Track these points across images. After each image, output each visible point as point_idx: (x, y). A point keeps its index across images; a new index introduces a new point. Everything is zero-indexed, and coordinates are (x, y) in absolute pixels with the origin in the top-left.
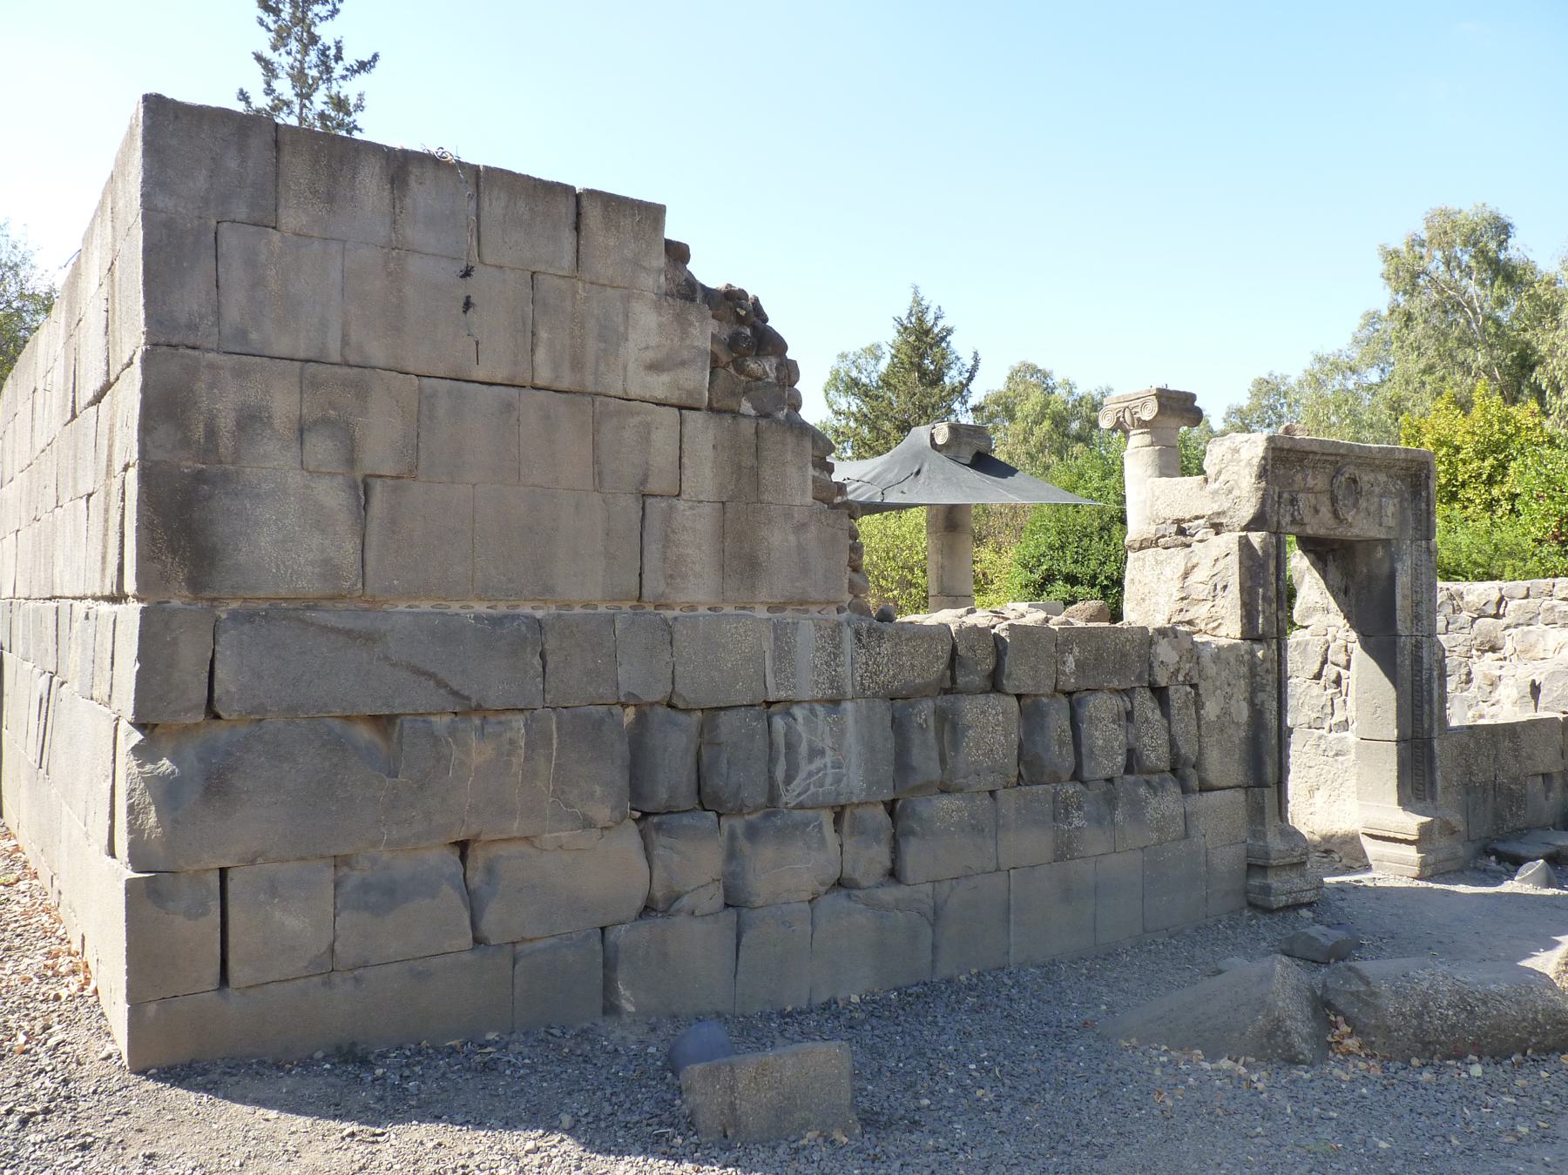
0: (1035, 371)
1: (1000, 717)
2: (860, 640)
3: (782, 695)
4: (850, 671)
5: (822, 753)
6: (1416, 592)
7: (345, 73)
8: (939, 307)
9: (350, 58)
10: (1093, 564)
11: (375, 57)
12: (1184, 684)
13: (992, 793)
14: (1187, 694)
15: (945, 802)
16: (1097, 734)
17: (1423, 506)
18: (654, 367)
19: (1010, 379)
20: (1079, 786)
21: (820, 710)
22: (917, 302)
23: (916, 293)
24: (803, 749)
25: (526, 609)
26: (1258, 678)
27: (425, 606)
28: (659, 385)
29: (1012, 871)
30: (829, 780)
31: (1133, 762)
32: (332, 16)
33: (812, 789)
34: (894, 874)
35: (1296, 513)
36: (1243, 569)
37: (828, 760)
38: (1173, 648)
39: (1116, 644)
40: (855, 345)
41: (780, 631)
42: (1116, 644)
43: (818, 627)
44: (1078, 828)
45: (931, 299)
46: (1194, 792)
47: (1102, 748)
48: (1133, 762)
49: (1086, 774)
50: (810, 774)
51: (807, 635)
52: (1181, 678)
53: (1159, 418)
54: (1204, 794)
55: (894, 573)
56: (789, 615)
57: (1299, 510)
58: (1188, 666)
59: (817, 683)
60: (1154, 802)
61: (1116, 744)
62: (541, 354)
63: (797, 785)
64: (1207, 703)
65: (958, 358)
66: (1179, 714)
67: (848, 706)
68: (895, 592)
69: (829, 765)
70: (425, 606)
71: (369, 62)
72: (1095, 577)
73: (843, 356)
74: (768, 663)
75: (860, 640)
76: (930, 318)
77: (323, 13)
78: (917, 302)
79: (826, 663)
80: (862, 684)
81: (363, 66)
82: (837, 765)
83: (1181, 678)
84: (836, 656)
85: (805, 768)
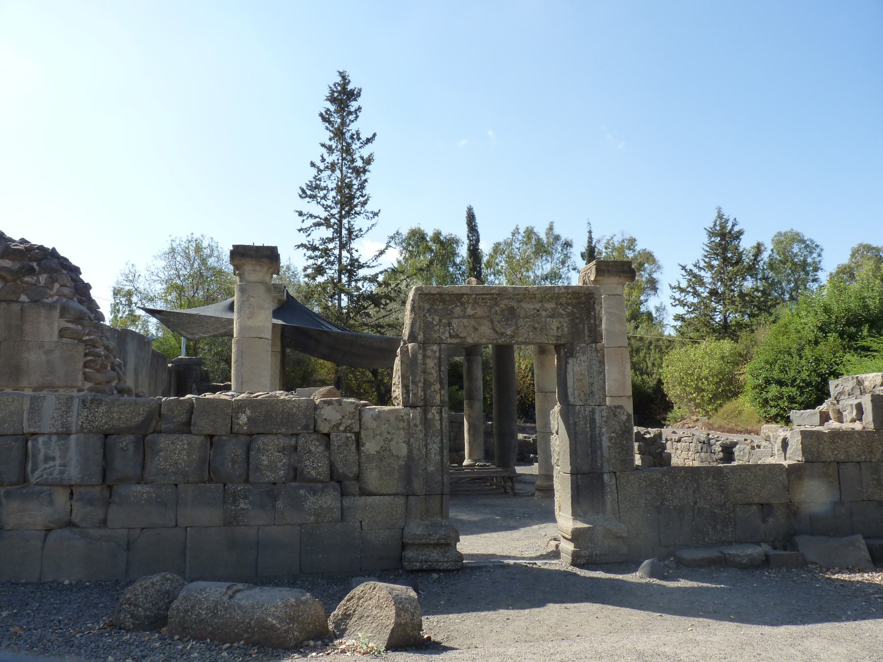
0: (868, 248)
1: (186, 446)
2: (85, 405)
3: (32, 430)
4: (76, 418)
5: (54, 459)
6: (591, 376)
7: (361, 145)
8: (735, 219)
9: (363, 137)
11: (374, 135)
12: (345, 431)
13: (176, 485)
14: (347, 438)
15: (139, 488)
16: (264, 458)
17: (592, 321)
19: (853, 255)
20: (247, 486)
21: (54, 438)
22: (720, 217)
23: (719, 212)
24: (41, 457)
26: (411, 429)
29: (188, 529)
30: (56, 472)
31: (296, 474)
32: (356, 119)
33: (45, 476)
34: (104, 523)
35: (451, 331)
36: (404, 366)
37: (58, 462)
38: (337, 411)
39: (283, 409)
41: (33, 400)
42: (283, 409)
43: (58, 398)
44: (243, 509)
45: (728, 213)
46: (355, 495)
47: (267, 466)
48: (296, 474)
49: (251, 479)
50: (45, 469)
51: (50, 403)
52: (342, 428)
53: (600, 278)
54: (363, 498)
55: (692, 383)
56: (44, 392)
57: (453, 329)
58: (349, 422)
59: (53, 425)
60: (313, 499)
61: (280, 465)
63: (37, 473)
64: (367, 444)
65: (817, 246)
66: (338, 449)
67: (73, 437)
69: (57, 465)
71: (371, 138)
72: (795, 380)
74: (25, 415)
75: (85, 405)
76: (730, 225)
78: (720, 217)
79: (61, 416)
80: (82, 426)
81: (368, 141)
82: (64, 465)
83: (342, 428)
84: (67, 412)
85: (42, 466)
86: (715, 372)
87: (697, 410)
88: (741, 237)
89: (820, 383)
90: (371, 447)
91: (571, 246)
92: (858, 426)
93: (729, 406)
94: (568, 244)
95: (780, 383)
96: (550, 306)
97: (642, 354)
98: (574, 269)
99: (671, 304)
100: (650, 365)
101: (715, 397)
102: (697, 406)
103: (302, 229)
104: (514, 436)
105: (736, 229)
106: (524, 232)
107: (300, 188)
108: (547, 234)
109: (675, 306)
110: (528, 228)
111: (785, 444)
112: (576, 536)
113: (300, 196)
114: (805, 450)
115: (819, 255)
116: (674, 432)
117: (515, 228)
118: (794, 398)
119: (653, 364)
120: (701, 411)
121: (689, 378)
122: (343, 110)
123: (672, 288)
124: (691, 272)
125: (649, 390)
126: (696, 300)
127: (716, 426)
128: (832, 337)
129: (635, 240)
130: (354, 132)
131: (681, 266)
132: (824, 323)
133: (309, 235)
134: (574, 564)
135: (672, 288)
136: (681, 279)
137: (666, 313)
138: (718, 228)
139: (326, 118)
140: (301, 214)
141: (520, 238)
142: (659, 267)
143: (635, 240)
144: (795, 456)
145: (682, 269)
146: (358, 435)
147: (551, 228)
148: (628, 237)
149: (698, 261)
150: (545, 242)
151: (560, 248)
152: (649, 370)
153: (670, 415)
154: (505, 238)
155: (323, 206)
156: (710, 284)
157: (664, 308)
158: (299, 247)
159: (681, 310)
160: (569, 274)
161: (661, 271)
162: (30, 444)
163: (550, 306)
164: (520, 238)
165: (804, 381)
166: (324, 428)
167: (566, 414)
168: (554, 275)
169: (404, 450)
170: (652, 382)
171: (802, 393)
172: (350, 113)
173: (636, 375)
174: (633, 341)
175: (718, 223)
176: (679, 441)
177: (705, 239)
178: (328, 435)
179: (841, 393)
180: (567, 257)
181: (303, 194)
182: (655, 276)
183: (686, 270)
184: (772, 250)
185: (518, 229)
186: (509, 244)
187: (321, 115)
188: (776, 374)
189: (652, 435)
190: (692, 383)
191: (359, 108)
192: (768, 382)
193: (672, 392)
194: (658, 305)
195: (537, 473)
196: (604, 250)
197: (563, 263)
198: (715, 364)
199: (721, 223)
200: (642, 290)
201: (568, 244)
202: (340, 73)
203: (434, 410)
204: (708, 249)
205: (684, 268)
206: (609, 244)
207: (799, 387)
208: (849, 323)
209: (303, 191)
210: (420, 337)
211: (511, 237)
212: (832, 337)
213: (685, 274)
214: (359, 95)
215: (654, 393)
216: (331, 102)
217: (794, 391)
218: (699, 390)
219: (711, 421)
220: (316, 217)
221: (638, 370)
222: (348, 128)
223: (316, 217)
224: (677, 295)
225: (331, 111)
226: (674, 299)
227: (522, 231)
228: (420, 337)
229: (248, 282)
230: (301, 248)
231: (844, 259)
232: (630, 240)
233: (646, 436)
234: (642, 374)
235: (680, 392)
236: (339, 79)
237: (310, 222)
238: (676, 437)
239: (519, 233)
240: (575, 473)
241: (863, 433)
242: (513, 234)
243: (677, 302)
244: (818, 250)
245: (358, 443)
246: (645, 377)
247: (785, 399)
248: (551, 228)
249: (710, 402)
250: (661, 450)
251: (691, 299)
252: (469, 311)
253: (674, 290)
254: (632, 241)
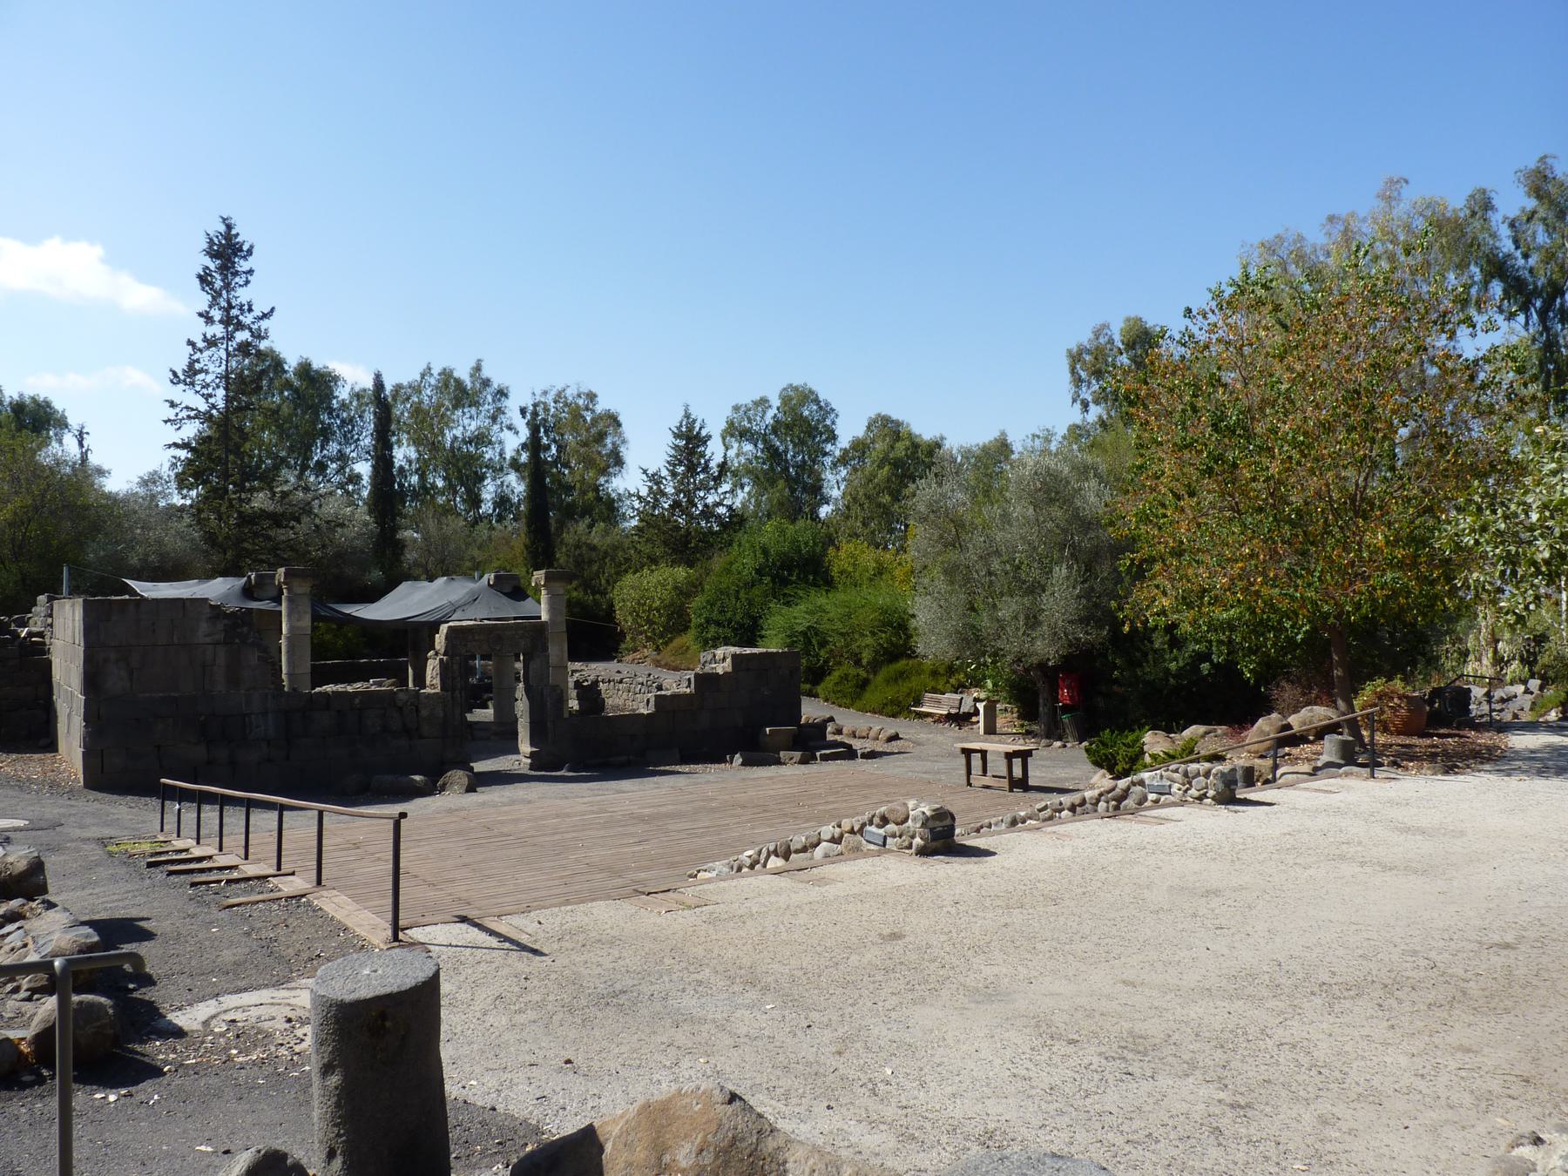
11: (273, 310)
18: (206, 636)
19: (868, 428)
22: (687, 416)
23: (687, 407)
25: (173, 694)
27: (147, 695)
28: (208, 640)
40: (746, 399)
62: (175, 637)
65: (833, 410)
70: (147, 695)
73: (736, 408)
76: (697, 426)
77: (242, 283)
78: (687, 416)
81: (265, 316)
86: (667, 602)
88: (708, 443)
90: (424, 713)
91: (506, 396)
92: (688, 690)
93: (678, 641)
94: (502, 393)
95: (718, 624)
96: (520, 632)
98: (510, 428)
100: (603, 582)
101: (667, 629)
102: (649, 639)
103: (169, 420)
105: (704, 433)
106: (440, 374)
107: (171, 370)
108: (471, 376)
110: (445, 369)
111: (648, 701)
112: (532, 756)
113: (172, 381)
114: (656, 705)
115: (833, 423)
116: (618, 672)
117: (425, 367)
119: (608, 581)
122: (227, 269)
127: (663, 663)
128: (767, 580)
129: (595, 396)
130: (244, 302)
133: (179, 428)
134: (530, 769)
138: (684, 429)
139: (204, 279)
140: (173, 405)
141: (433, 381)
143: (595, 396)
144: (651, 709)
146: (417, 707)
147: (478, 369)
148: (586, 391)
150: (469, 388)
151: (490, 398)
154: (410, 380)
155: (203, 395)
156: (672, 495)
158: (170, 446)
160: (502, 435)
162: (247, 719)
163: (520, 632)
164: (433, 381)
165: (738, 623)
166: (400, 704)
167: (528, 690)
168: (481, 439)
169: (441, 714)
171: (736, 635)
172: (236, 274)
175: (684, 423)
176: (621, 682)
177: (670, 439)
178: (401, 708)
179: (706, 662)
180: (500, 411)
181: (175, 379)
184: (778, 409)
185: (430, 369)
186: (417, 389)
187: (200, 277)
188: (715, 615)
191: (251, 272)
192: (708, 621)
193: (624, 618)
195: (492, 719)
196: (552, 404)
197: (494, 419)
198: (667, 595)
199: (688, 423)
200: (604, 471)
201: (502, 393)
202: (224, 220)
203: (457, 692)
204: (673, 452)
206: (560, 397)
207: (734, 630)
208: (782, 567)
209: (175, 374)
210: (450, 653)
211: (419, 379)
213: (646, 479)
214: (250, 252)
216: (211, 257)
218: (650, 622)
219: (659, 658)
220: (193, 410)
222: (236, 295)
223: (193, 410)
225: (211, 271)
227: (435, 372)
228: (450, 653)
229: (296, 594)
230: (172, 448)
231: (859, 431)
232: (588, 395)
236: (222, 228)
237: (184, 414)
238: (618, 678)
239: (432, 375)
240: (532, 723)
241: (690, 695)
242: (423, 376)
244: (833, 416)
245: (417, 711)
246: (598, 597)
248: (478, 369)
249: (662, 636)
252: (477, 637)
254: (592, 397)
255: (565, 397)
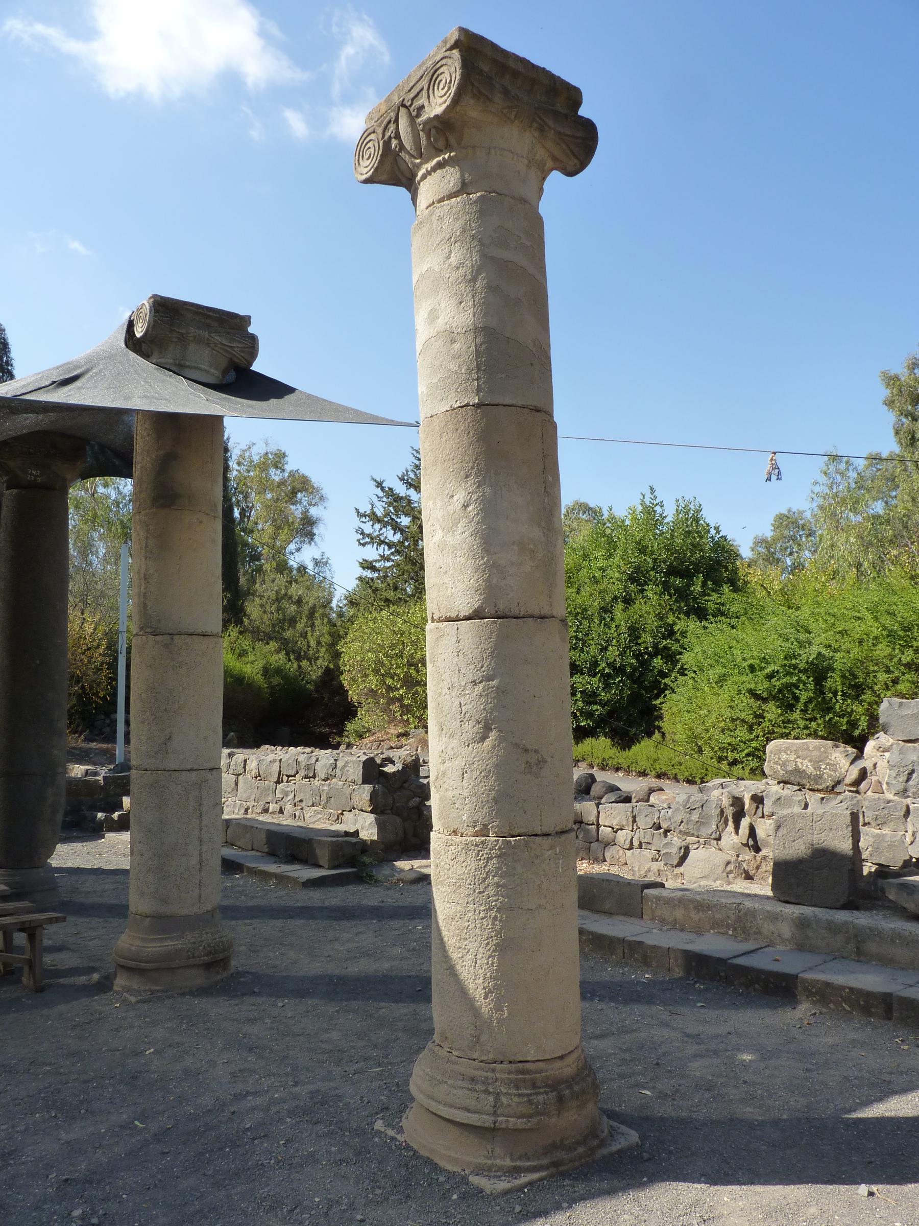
10: (593, 650)
68: (401, 692)
72: (595, 664)
87: (405, 717)
89: (635, 669)
97: (299, 626)
99: (358, 540)
100: (313, 643)
104: (54, 769)
109: (364, 545)
118: (594, 694)
119: (319, 643)
120: (411, 720)
121: (393, 662)
123: (361, 515)
124: (390, 493)
125: (308, 686)
126: (398, 537)
128: (651, 591)
129: (284, 455)
131: (375, 481)
132: (637, 569)
135: (361, 515)
136: (375, 499)
137: (329, 570)
142: (322, 498)
143: (284, 455)
145: (377, 487)
149: (407, 471)
152: (311, 652)
153: (350, 727)
157: (327, 563)
159: (371, 553)
161: (325, 504)
170: (314, 672)
171: (607, 686)
173: (290, 660)
174: (285, 604)
182: (314, 512)
183: (383, 489)
189: (398, 767)
190: (398, 672)
194: (318, 557)
205: (379, 485)
207: (606, 677)
212: (651, 591)
213: (381, 494)
215: (317, 690)
217: (595, 682)
221: (293, 651)
224: (368, 528)
226: (362, 533)
232: (276, 454)
233: (386, 769)
234: (299, 659)
235: (376, 686)
243: (367, 540)
246: (305, 663)
247: (579, 696)
250: (417, 800)
251: (391, 535)
253: (363, 519)
255: (250, 456)
